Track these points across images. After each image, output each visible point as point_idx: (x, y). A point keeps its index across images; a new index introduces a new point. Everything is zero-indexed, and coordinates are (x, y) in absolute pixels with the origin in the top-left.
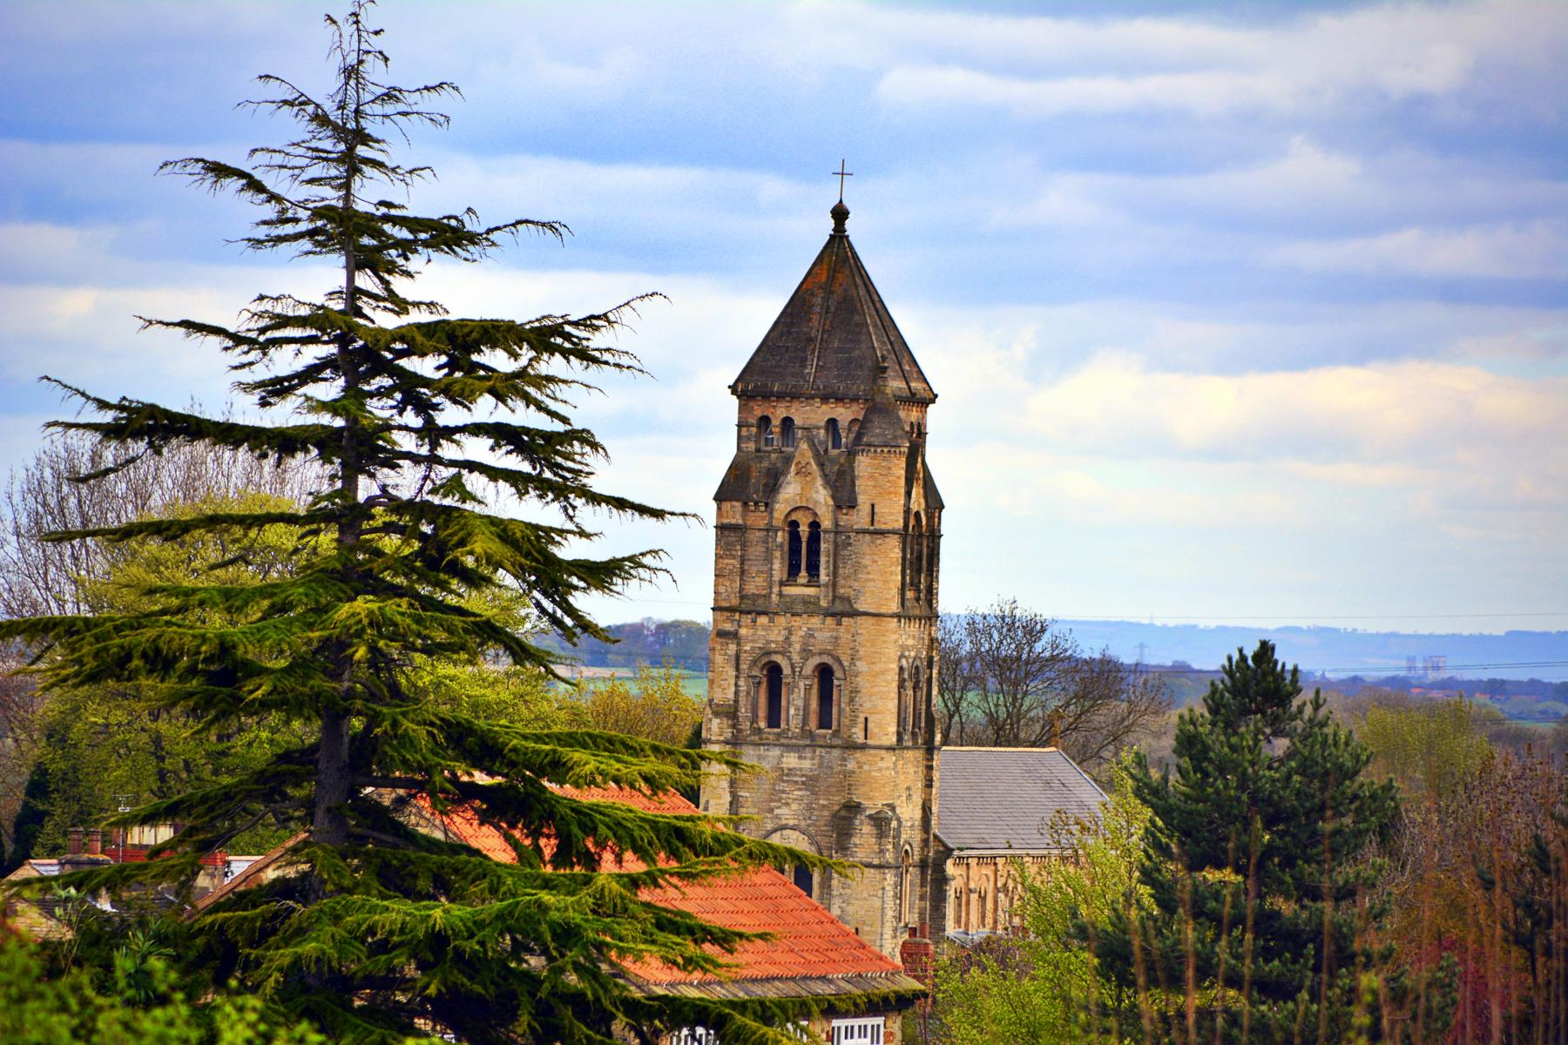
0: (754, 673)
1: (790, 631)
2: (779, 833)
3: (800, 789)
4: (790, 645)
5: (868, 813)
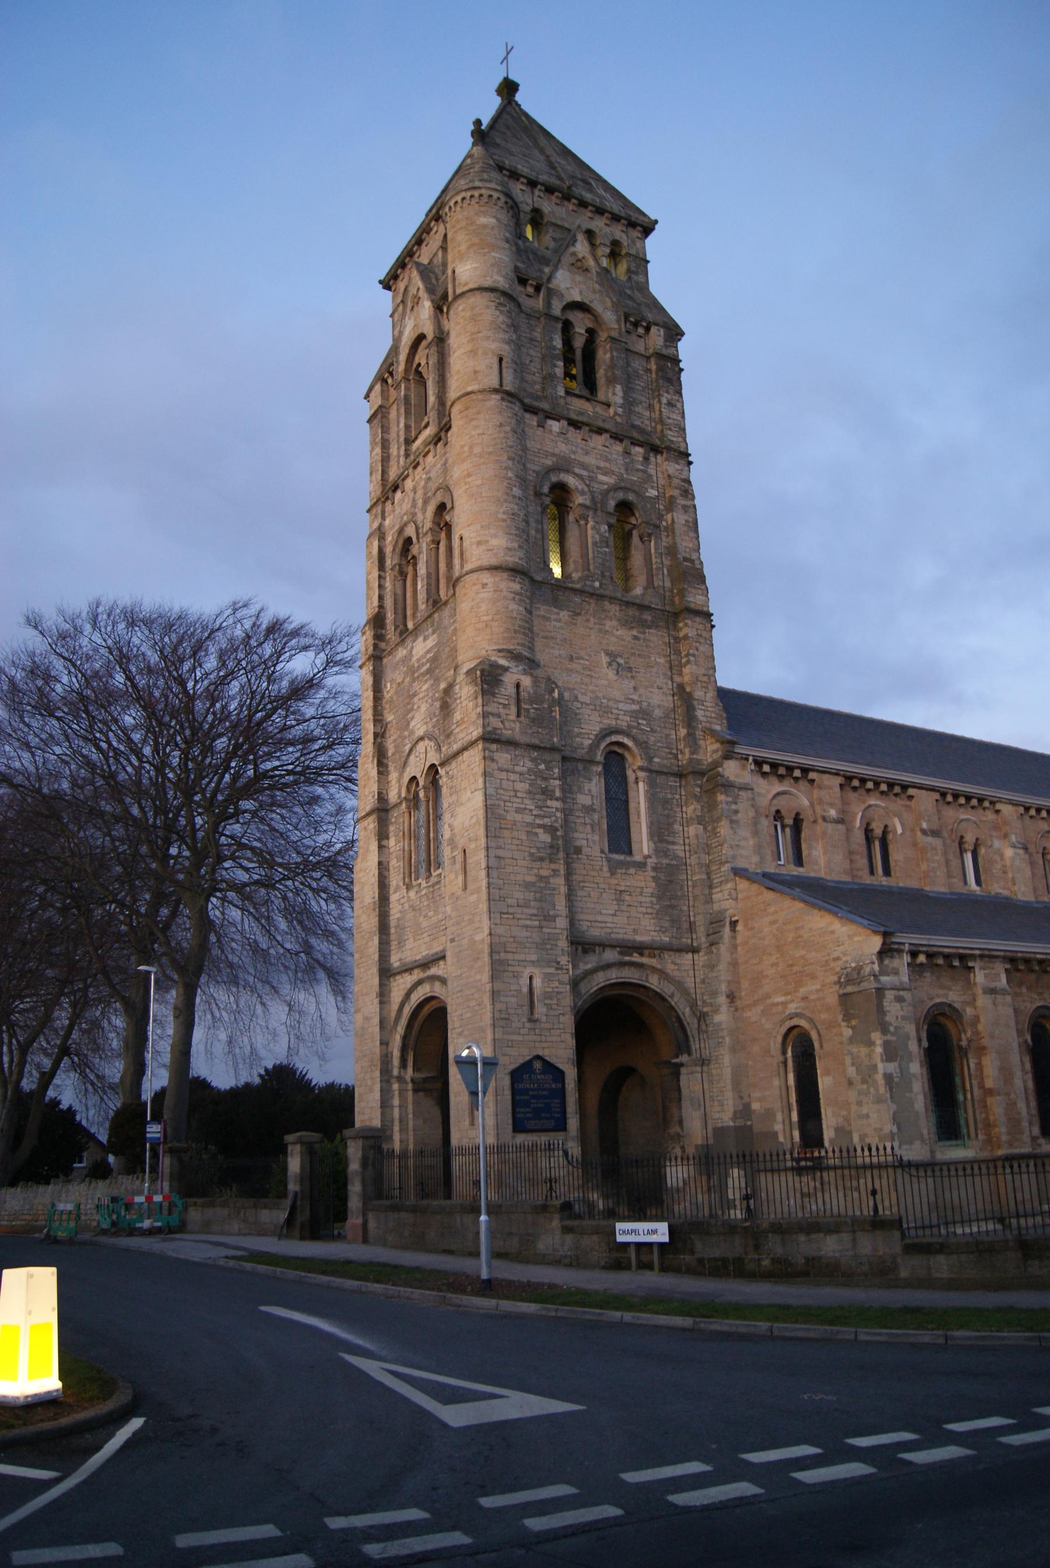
3: (426, 681)
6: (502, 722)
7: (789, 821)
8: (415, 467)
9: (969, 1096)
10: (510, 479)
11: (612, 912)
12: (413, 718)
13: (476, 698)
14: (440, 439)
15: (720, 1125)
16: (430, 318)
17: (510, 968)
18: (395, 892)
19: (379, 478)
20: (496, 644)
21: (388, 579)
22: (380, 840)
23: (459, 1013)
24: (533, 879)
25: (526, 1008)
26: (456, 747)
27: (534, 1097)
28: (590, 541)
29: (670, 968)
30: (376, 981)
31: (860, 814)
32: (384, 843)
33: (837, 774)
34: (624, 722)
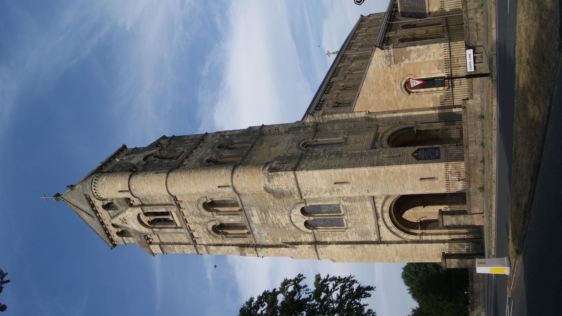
0: (221, 238)
1: (195, 223)
2: (295, 223)
3: (269, 215)
4: (202, 223)
5: (267, 183)
6: (289, 167)
7: (337, 105)
8: (187, 222)
9: (428, 37)
10: (201, 169)
11: (362, 144)
12: (282, 224)
13: (279, 175)
14: (179, 204)
15: (438, 117)
17: (380, 162)
18: (347, 237)
19: (186, 246)
20: (260, 171)
21: (226, 242)
22: (327, 244)
23: (395, 187)
24: (348, 158)
25: (394, 158)
26: (296, 189)
27: (427, 155)
28: (229, 154)
29: (383, 131)
30: (382, 246)
31: (337, 91)
32: (328, 243)
33: (323, 95)
34: (295, 144)
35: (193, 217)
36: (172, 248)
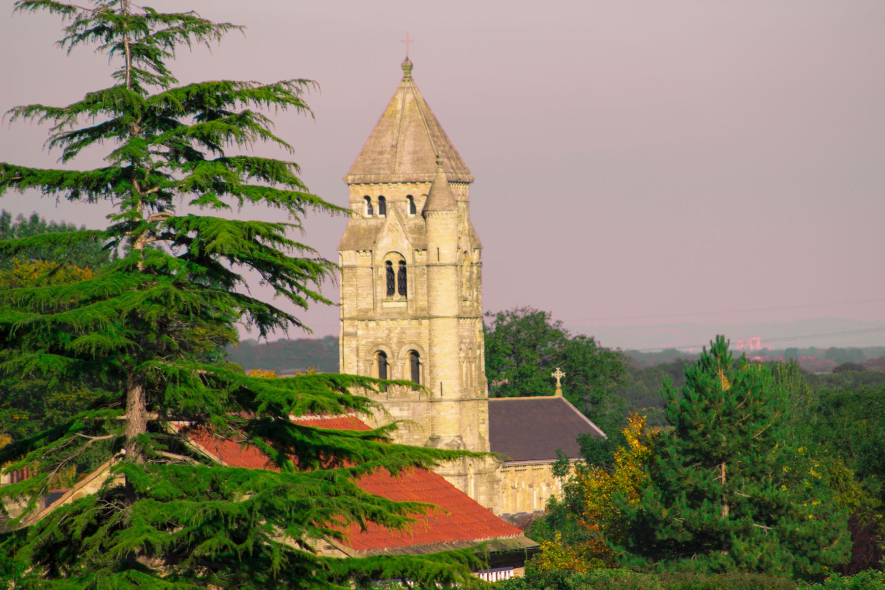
4: (390, 340)
16: (409, 249)
35: (397, 331)
36: (352, 283)
